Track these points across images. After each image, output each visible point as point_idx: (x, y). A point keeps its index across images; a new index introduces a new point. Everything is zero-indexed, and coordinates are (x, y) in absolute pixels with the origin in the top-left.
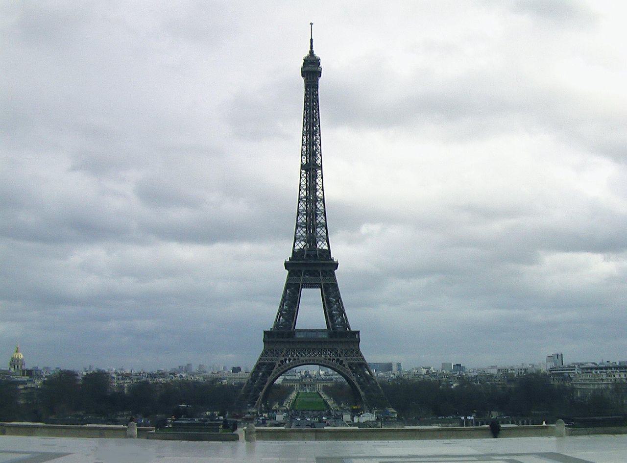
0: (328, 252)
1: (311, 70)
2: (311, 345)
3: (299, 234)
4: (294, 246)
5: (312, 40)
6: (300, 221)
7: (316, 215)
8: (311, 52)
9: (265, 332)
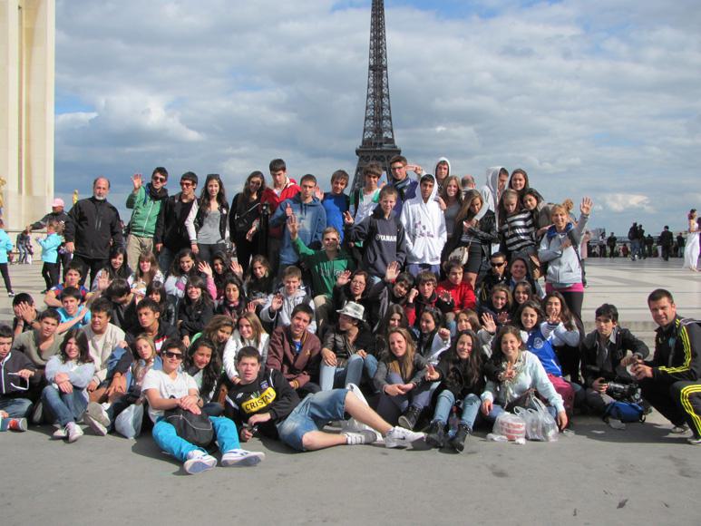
0: (391, 141)
4: (364, 136)
7: (382, 109)
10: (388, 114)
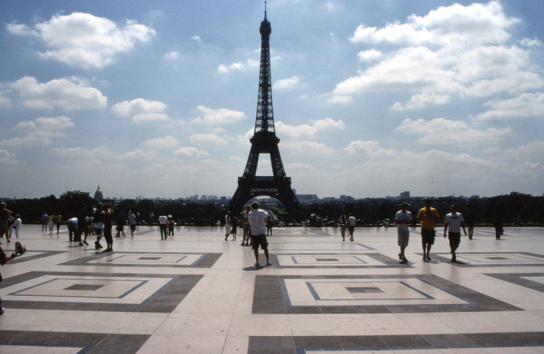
1: (265, 29)
2: (264, 184)
3: (258, 123)
5: (266, 12)
6: (259, 116)
7: (267, 113)
8: (265, 19)
9: (239, 178)
10: (271, 116)
